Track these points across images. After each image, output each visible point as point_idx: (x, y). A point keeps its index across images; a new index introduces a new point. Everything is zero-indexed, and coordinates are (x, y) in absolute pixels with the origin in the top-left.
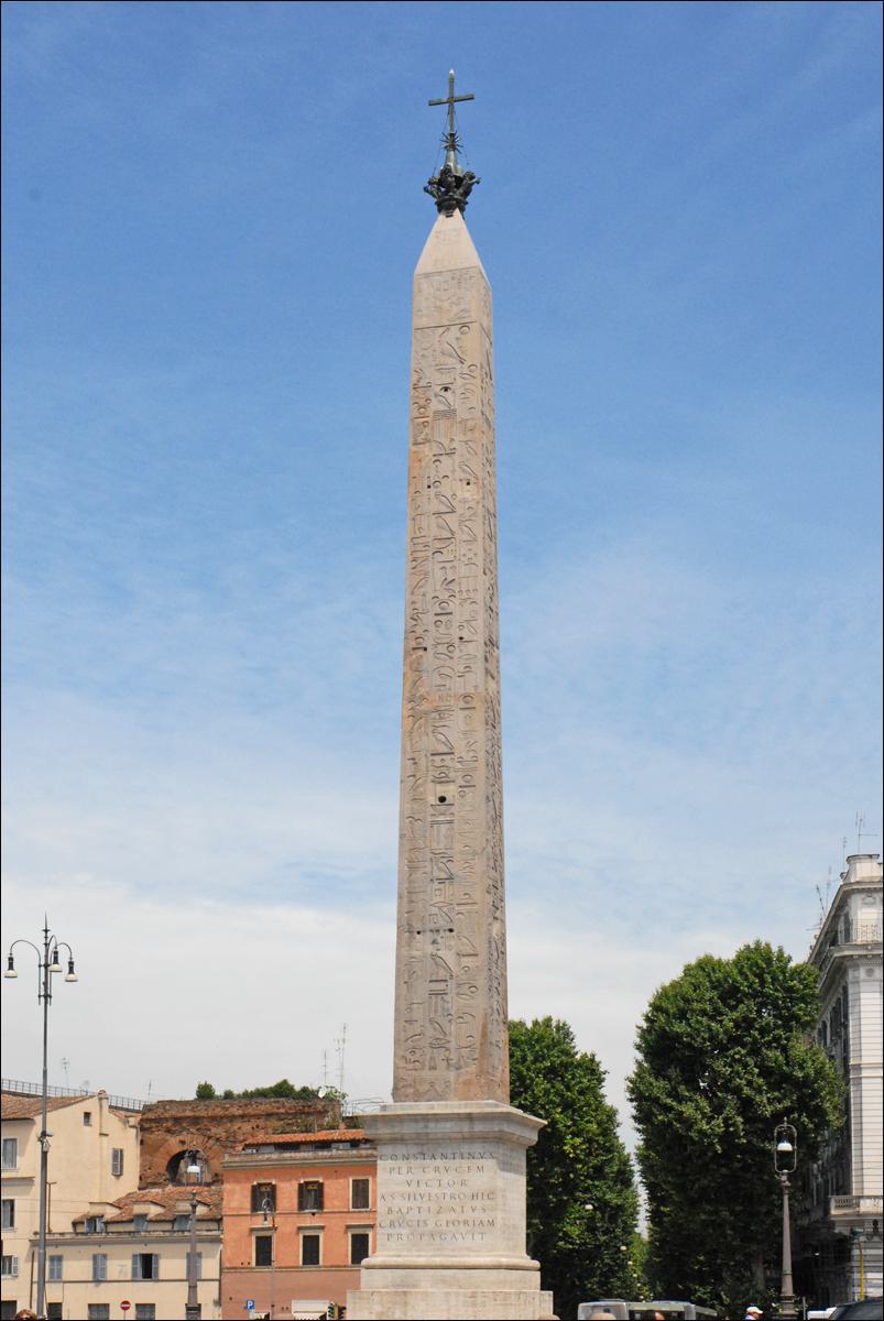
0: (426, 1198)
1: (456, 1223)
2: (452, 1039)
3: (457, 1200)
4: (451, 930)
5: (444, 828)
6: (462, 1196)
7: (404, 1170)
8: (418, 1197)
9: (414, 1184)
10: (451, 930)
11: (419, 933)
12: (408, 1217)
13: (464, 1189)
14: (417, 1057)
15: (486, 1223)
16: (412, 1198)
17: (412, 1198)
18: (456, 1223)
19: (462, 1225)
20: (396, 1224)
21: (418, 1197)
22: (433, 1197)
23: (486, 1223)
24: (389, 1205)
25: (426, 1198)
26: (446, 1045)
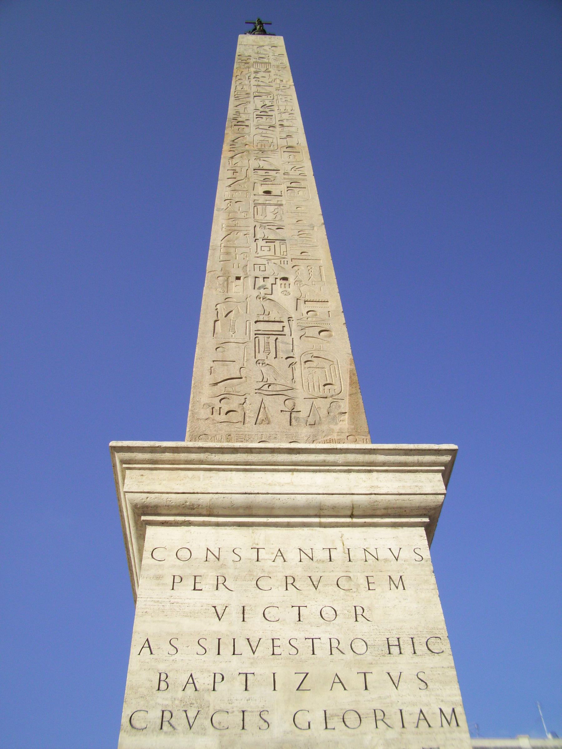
0: (264, 650)
1: (352, 719)
2: (298, 386)
3: (349, 654)
4: (285, 279)
5: (272, 208)
6: (360, 647)
7: (207, 584)
8: (242, 646)
9: (234, 614)
10: (285, 279)
11: (238, 278)
12: (211, 697)
13: (362, 628)
14: (233, 406)
15: (435, 720)
16: (226, 650)
17: (226, 650)
18: (352, 719)
19: (369, 723)
20: (180, 721)
21: (242, 646)
22: (283, 649)
23: (435, 720)
24: (162, 667)
25: (264, 650)
26: (289, 393)
